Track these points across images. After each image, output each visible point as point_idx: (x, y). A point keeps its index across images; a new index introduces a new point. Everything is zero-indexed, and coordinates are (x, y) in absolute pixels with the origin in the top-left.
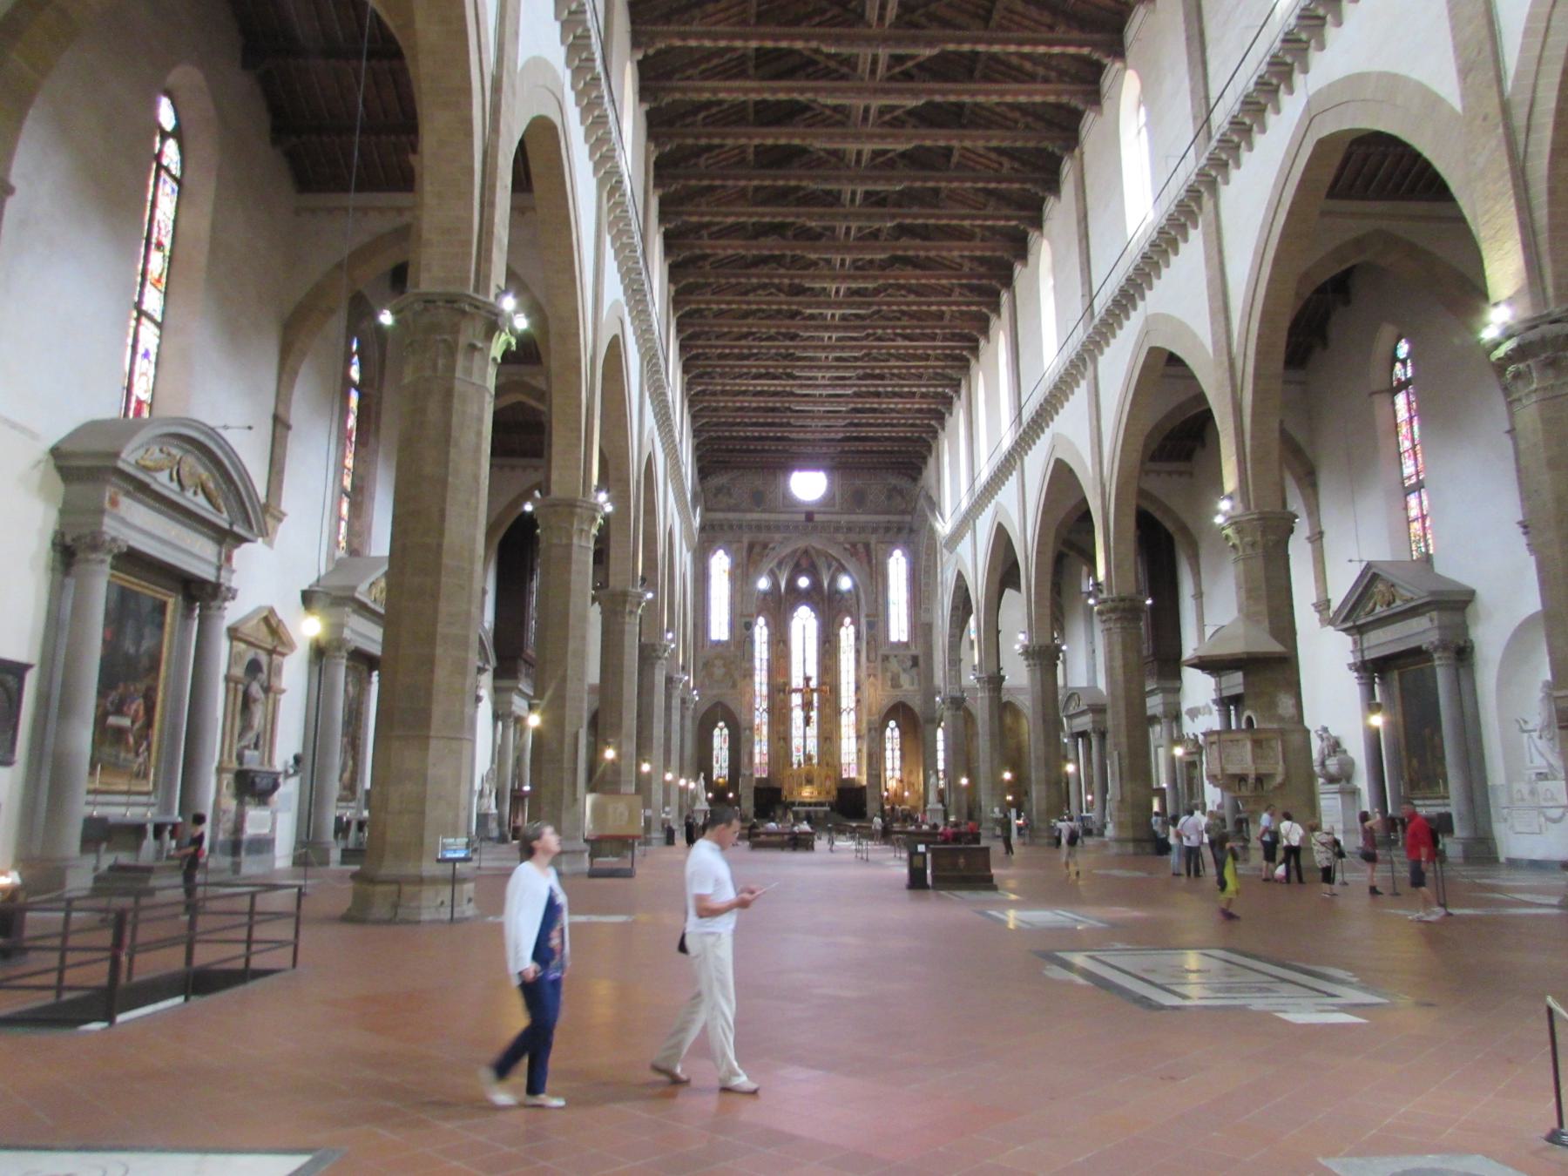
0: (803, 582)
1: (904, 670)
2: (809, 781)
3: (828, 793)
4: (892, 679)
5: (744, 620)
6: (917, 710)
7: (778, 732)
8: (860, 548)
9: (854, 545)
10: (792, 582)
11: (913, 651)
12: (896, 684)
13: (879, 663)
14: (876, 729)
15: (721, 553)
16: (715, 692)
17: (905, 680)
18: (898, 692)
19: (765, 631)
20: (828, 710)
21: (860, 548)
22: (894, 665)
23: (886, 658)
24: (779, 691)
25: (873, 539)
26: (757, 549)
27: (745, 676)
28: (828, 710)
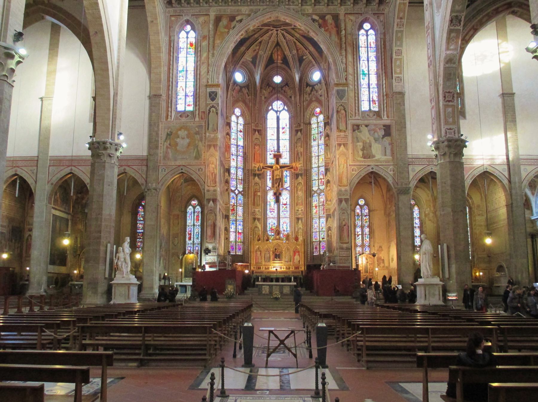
0: (278, 79)
1: (376, 140)
2: (277, 256)
3: (297, 268)
4: (363, 149)
5: (209, 90)
6: (390, 180)
7: (254, 213)
8: (329, 18)
9: (323, 17)
10: (267, 82)
11: (386, 120)
12: (367, 155)
13: (349, 133)
14: (346, 200)
15: (188, 28)
16: (178, 163)
17: (377, 150)
18: (368, 162)
19: (241, 121)
20: (300, 193)
21: (329, 18)
22: (365, 135)
23: (356, 127)
24: (255, 175)
25: (342, 11)
26: (224, 22)
27: (209, 146)
28: (300, 193)
